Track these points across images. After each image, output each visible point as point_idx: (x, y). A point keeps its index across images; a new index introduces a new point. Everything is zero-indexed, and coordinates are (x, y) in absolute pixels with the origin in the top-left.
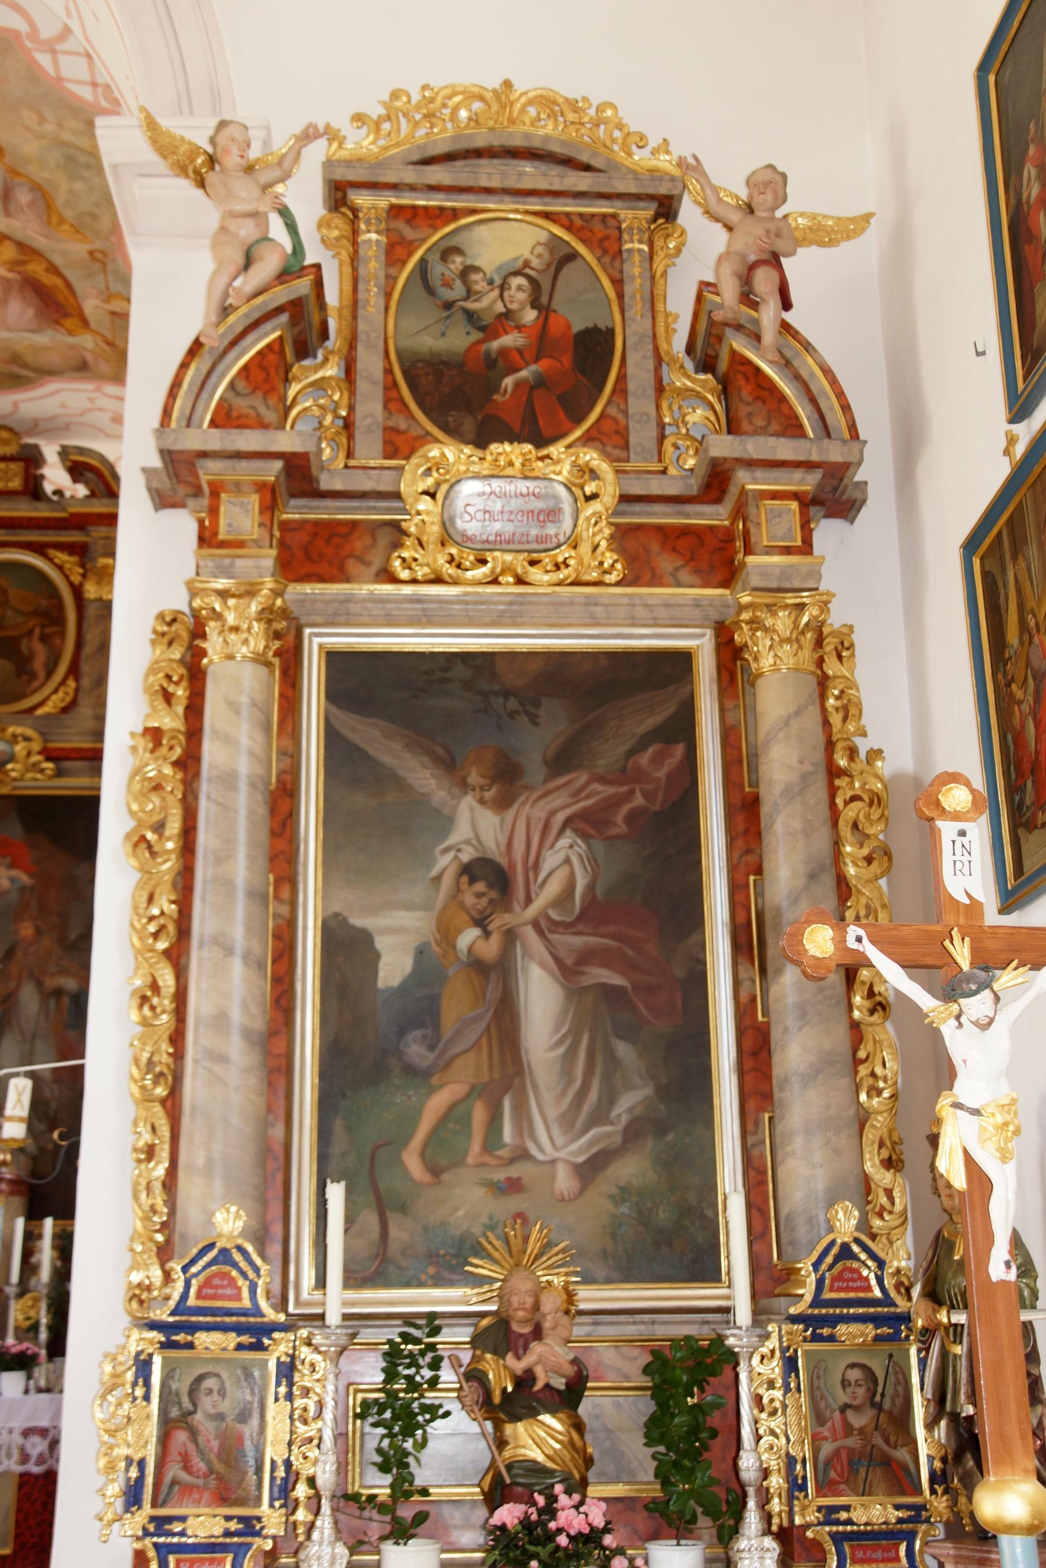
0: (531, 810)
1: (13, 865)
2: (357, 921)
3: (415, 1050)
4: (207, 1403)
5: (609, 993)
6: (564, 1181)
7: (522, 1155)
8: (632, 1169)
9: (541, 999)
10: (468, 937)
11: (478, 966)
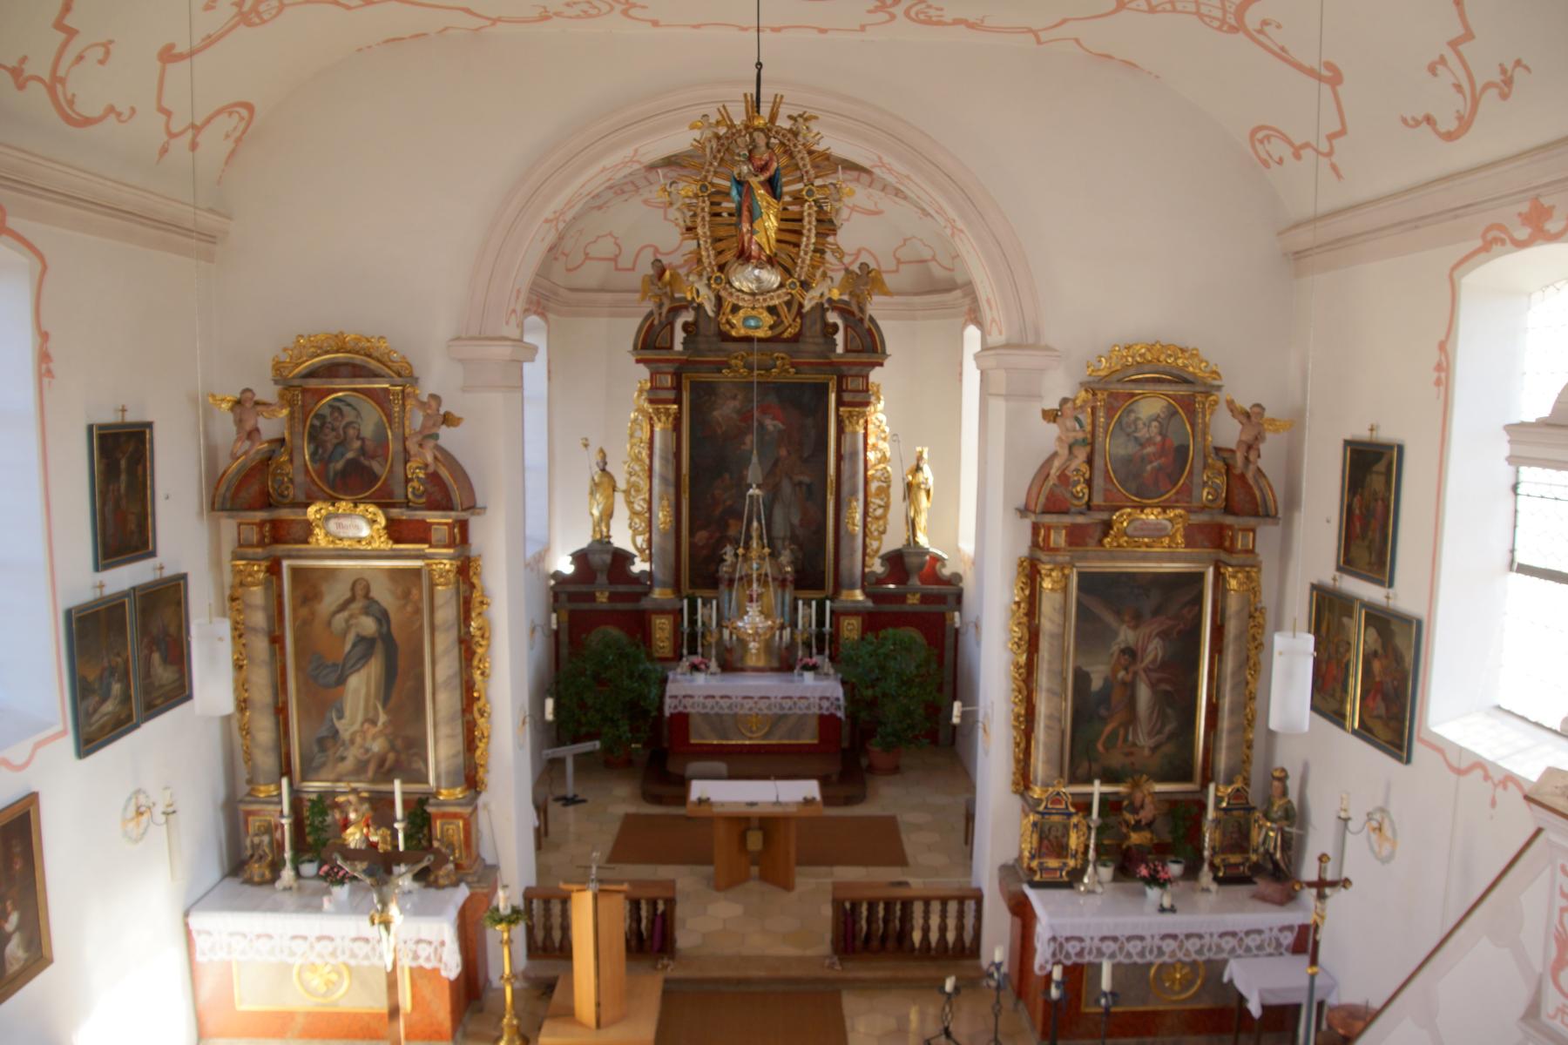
0: (1145, 630)
1: (774, 418)
2: (1085, 669)
3: (1103, 712)
4: (1053, 833)
5: (1166, 693)
6: (1147, 752)
7: (1134, 745)
8: (1168, 749)
9: (1144, 694)
10: (1121, 674)
11: (1124, 683)
